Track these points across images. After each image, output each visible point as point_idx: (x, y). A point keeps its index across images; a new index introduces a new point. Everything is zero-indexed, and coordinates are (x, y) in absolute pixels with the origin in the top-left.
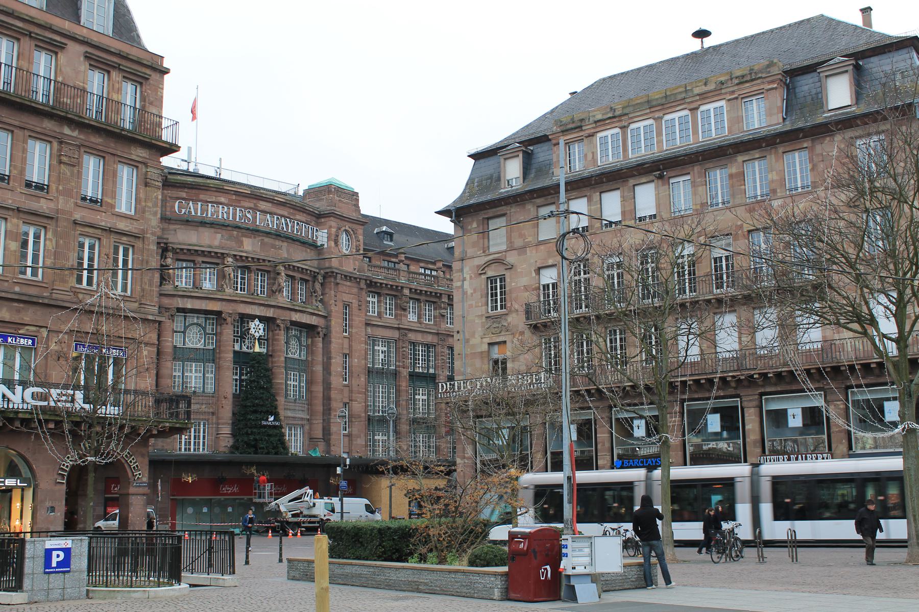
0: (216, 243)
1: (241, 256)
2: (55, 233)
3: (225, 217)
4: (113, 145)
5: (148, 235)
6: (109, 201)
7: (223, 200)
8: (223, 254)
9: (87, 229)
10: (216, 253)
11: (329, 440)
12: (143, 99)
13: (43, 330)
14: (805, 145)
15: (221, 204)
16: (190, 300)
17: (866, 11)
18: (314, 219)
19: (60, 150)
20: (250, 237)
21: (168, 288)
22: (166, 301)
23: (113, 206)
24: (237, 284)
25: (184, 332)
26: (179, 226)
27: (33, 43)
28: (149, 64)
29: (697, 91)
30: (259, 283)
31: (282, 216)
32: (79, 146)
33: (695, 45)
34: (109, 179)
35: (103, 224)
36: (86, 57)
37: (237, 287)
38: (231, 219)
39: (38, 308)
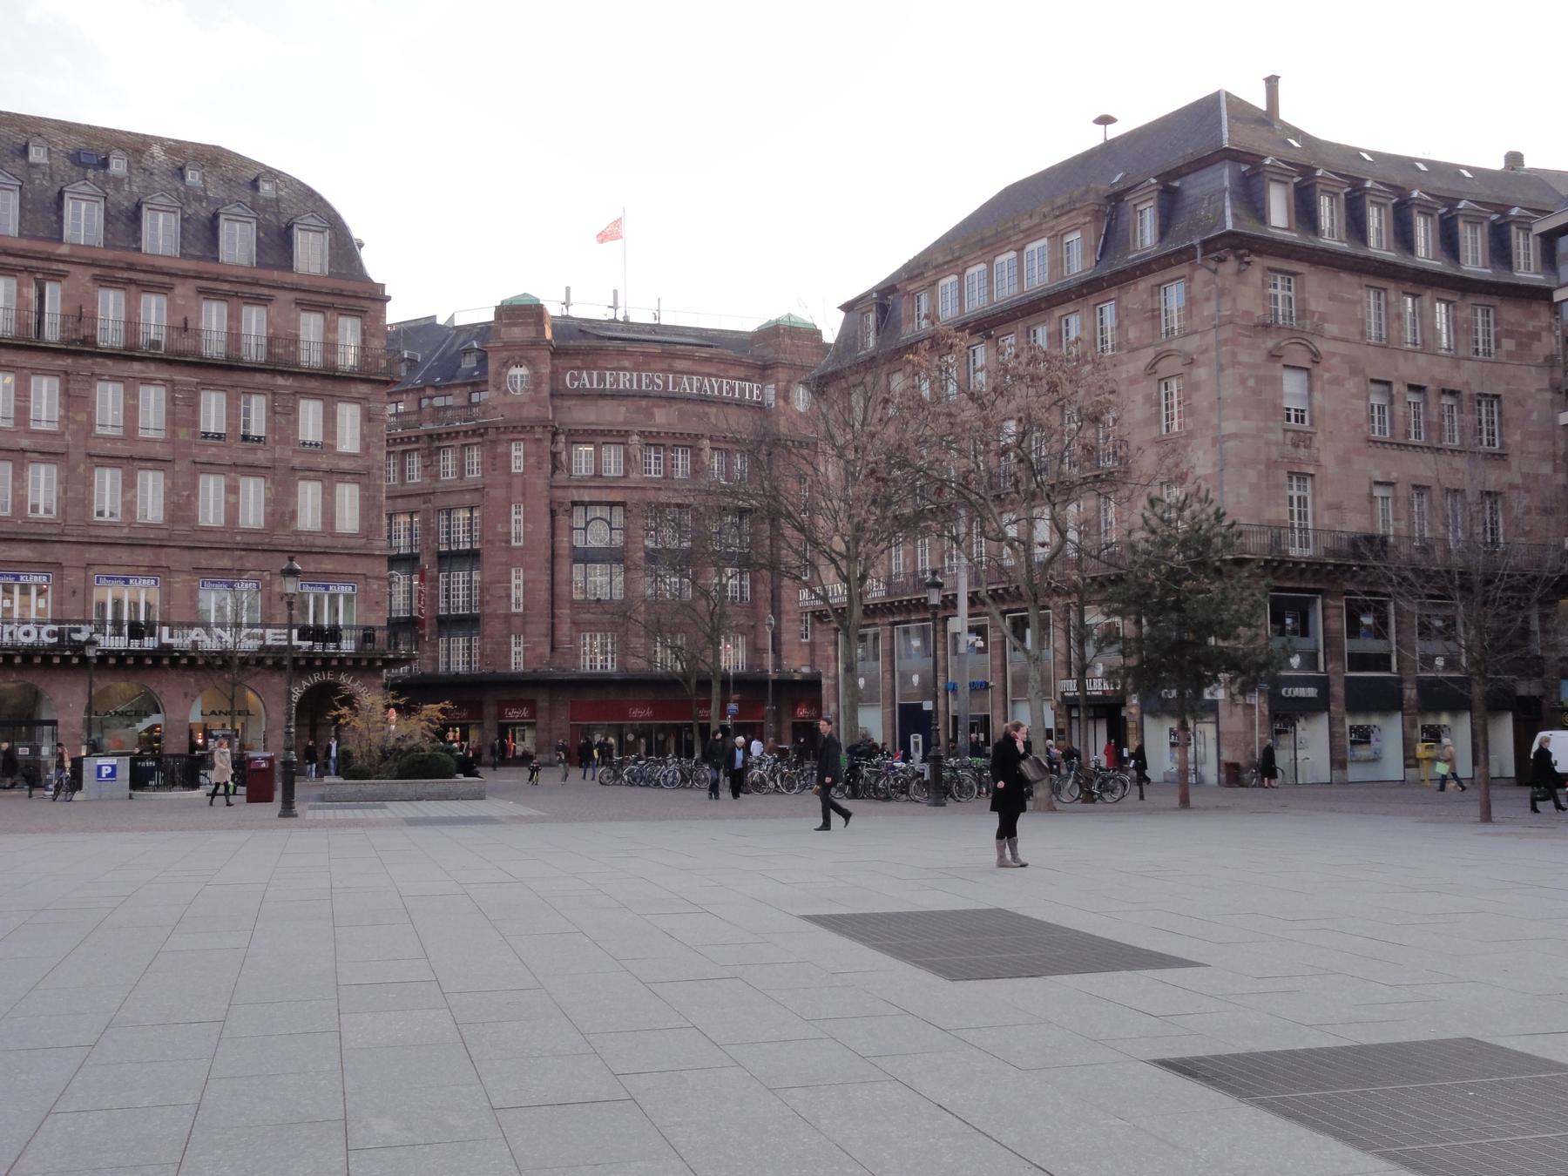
0: (620, 418)
1: (651, 433)
2: (273, 482)
3: (628, 385)
4: (330, 387)
5: (374, 471)
6: (330, 442)
7: (626, 364)
8: (626, 431)
9: (308, 473)
10: (618, 431)
11: (780, 650)
12: (364, 333)
13: (265, 573)
14: (1112, 297)
15: (624, 369)
16: (587, 491)
17: (1272, 83)
18: (759, 371)
19: (274, 401)
20: (664, 406)
21: (561, 477)
22: (559, 494)
23: (333, 447)
24: (650, 465)
25: (585, 529)
26: (574, 402)
27: (241, 301)
28: (367, 295)
29: (1024, 226)
30: (680, 462)
31: (704, 375)
32: (295, 393)
33: (1094, 138)
34: (330, 420)
35: (324, 466)
36: (297, 303)
37: (650, 470)
38: (635, 387)
39: (260, 554)
